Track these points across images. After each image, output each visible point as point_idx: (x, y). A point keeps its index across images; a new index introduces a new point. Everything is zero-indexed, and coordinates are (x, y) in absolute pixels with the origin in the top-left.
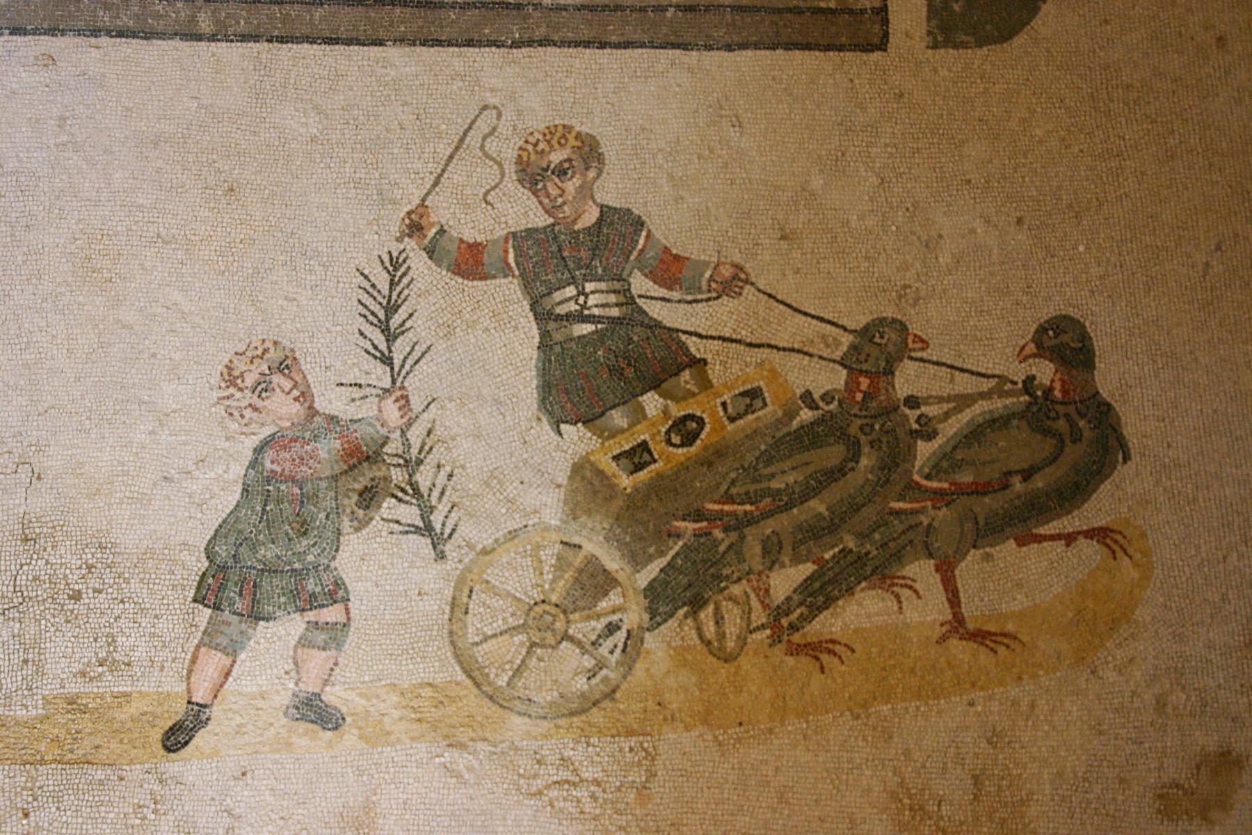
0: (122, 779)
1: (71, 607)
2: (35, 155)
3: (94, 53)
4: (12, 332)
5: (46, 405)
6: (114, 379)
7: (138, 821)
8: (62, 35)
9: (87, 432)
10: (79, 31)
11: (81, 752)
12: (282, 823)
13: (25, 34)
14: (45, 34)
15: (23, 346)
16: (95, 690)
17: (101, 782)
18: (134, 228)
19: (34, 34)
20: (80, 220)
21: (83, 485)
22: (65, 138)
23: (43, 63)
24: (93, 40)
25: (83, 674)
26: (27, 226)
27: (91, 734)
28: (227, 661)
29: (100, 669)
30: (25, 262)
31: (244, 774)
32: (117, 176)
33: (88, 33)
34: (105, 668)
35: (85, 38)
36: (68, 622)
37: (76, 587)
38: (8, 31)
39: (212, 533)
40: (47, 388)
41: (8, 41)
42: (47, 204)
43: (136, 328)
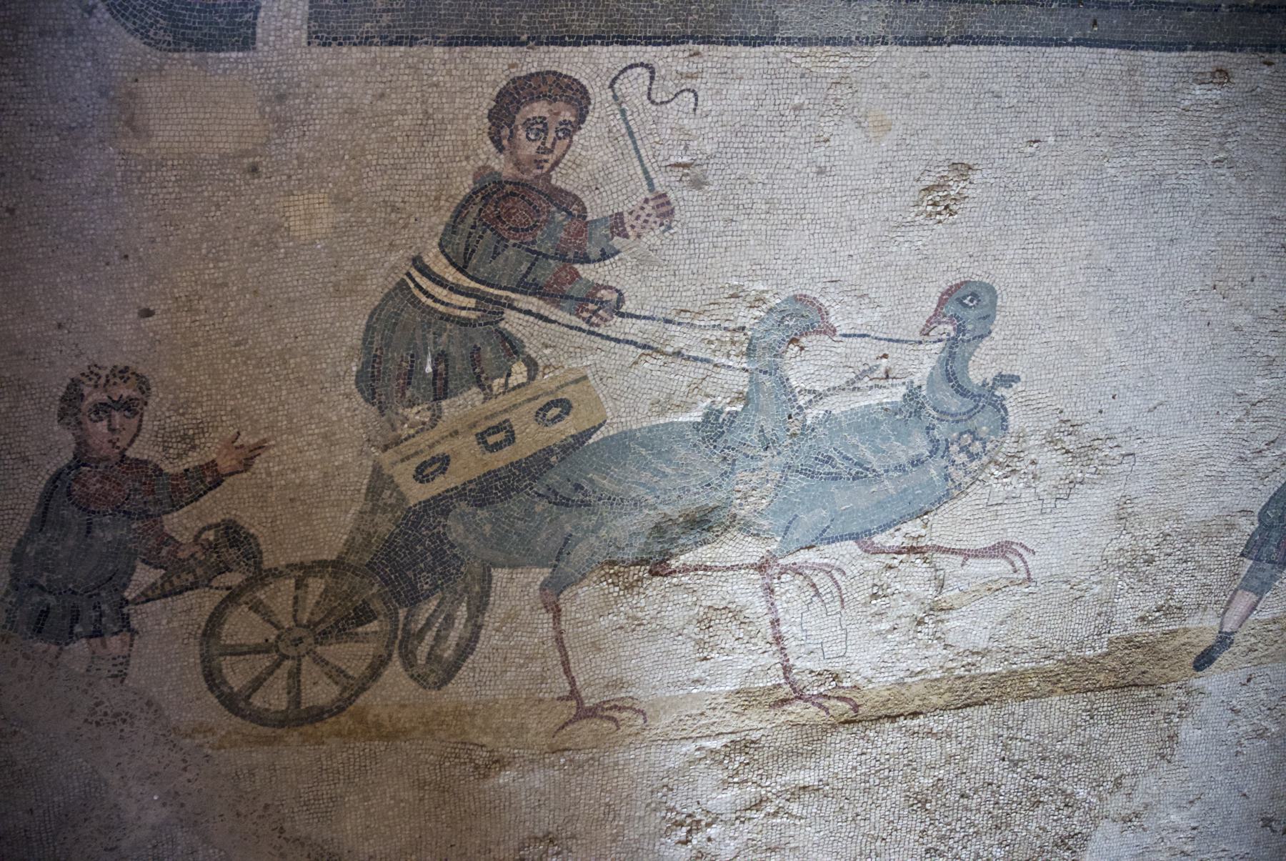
0: (1159, 695)
1: (1144, 569)
2: (1193, 172)
3: (1267, 71)
4: (1140, 340)
5: (1156, 402)
6: (1218, 376)
7: (1166, 725)
8: (1240, 51)
9: (1185, 423)
10: (1256, 46)
11: (1130, 678)
12: (1268, 712)
13: (1207, 50)
14: (1224, 49)
15: (1147, 352)
16: (1150, 630)
17: (1143, 700)
18: (1264, 239)
19: (1215, 49)
20: (1219, 233)
21: (1173, 468)
22: (1222, 155)
23: (1218, 80)
24: (1267, 56)
25: (1143, 619)
26: (1172, 240)
27: (1141, 663)
28: (1255, 598)
29: (1157, 614)
30: (1163, 274)
31: (1249, 680)
32: (1261, 191)
33: (1264, 48)
34: (1162, 613)
35: (1261, 54)
36: (1139, 581)
37: (1152, 552)
38: (1190, 46)
39: (1267, 500)
40: (1160, 387)
41: (1189, 57)
42: (1194, 218)
43: (1245, 329)
